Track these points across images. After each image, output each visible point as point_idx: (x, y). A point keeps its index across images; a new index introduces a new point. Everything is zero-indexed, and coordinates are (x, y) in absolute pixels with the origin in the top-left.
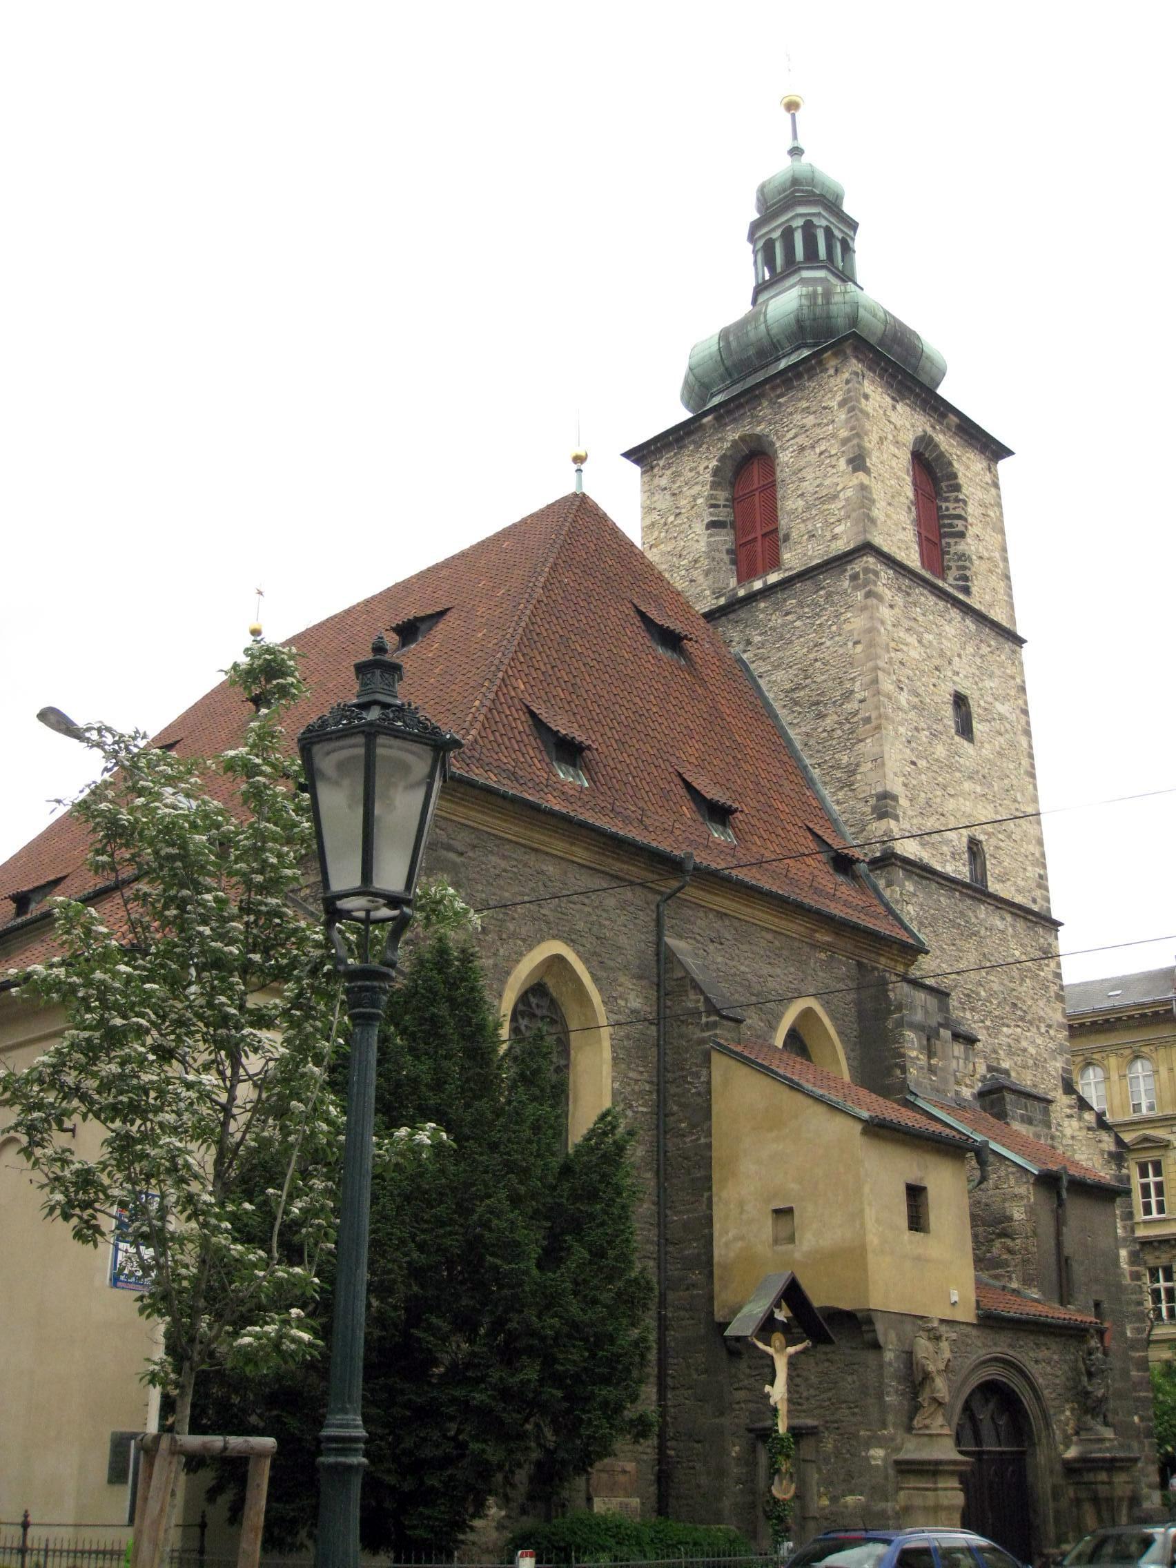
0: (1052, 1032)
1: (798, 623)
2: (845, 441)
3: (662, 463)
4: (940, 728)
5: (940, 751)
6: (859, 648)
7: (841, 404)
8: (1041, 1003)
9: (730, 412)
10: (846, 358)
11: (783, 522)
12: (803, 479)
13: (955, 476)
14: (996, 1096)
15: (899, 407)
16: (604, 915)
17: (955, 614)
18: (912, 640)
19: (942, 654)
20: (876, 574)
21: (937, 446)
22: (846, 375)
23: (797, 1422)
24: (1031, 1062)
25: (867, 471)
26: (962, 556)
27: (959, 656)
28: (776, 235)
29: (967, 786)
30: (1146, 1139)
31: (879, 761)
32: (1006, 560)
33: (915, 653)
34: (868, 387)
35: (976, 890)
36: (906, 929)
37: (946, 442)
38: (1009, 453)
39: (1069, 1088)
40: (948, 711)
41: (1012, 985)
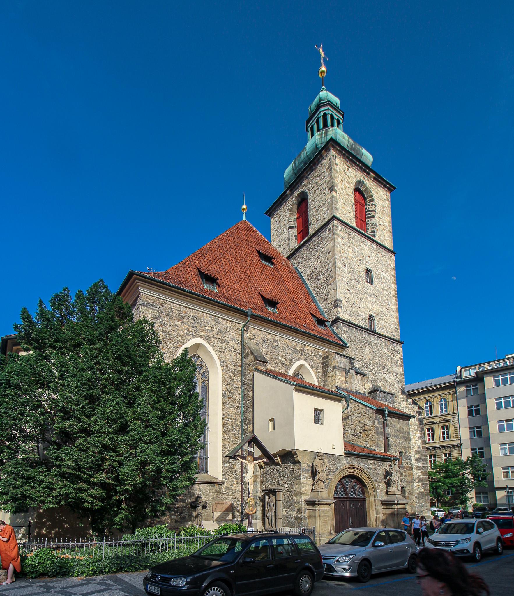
4: (360, 279)
6: (331, 253)
17: (368, 242)
27: (369, 257)
29: (369, 299)
31: (335, 289)
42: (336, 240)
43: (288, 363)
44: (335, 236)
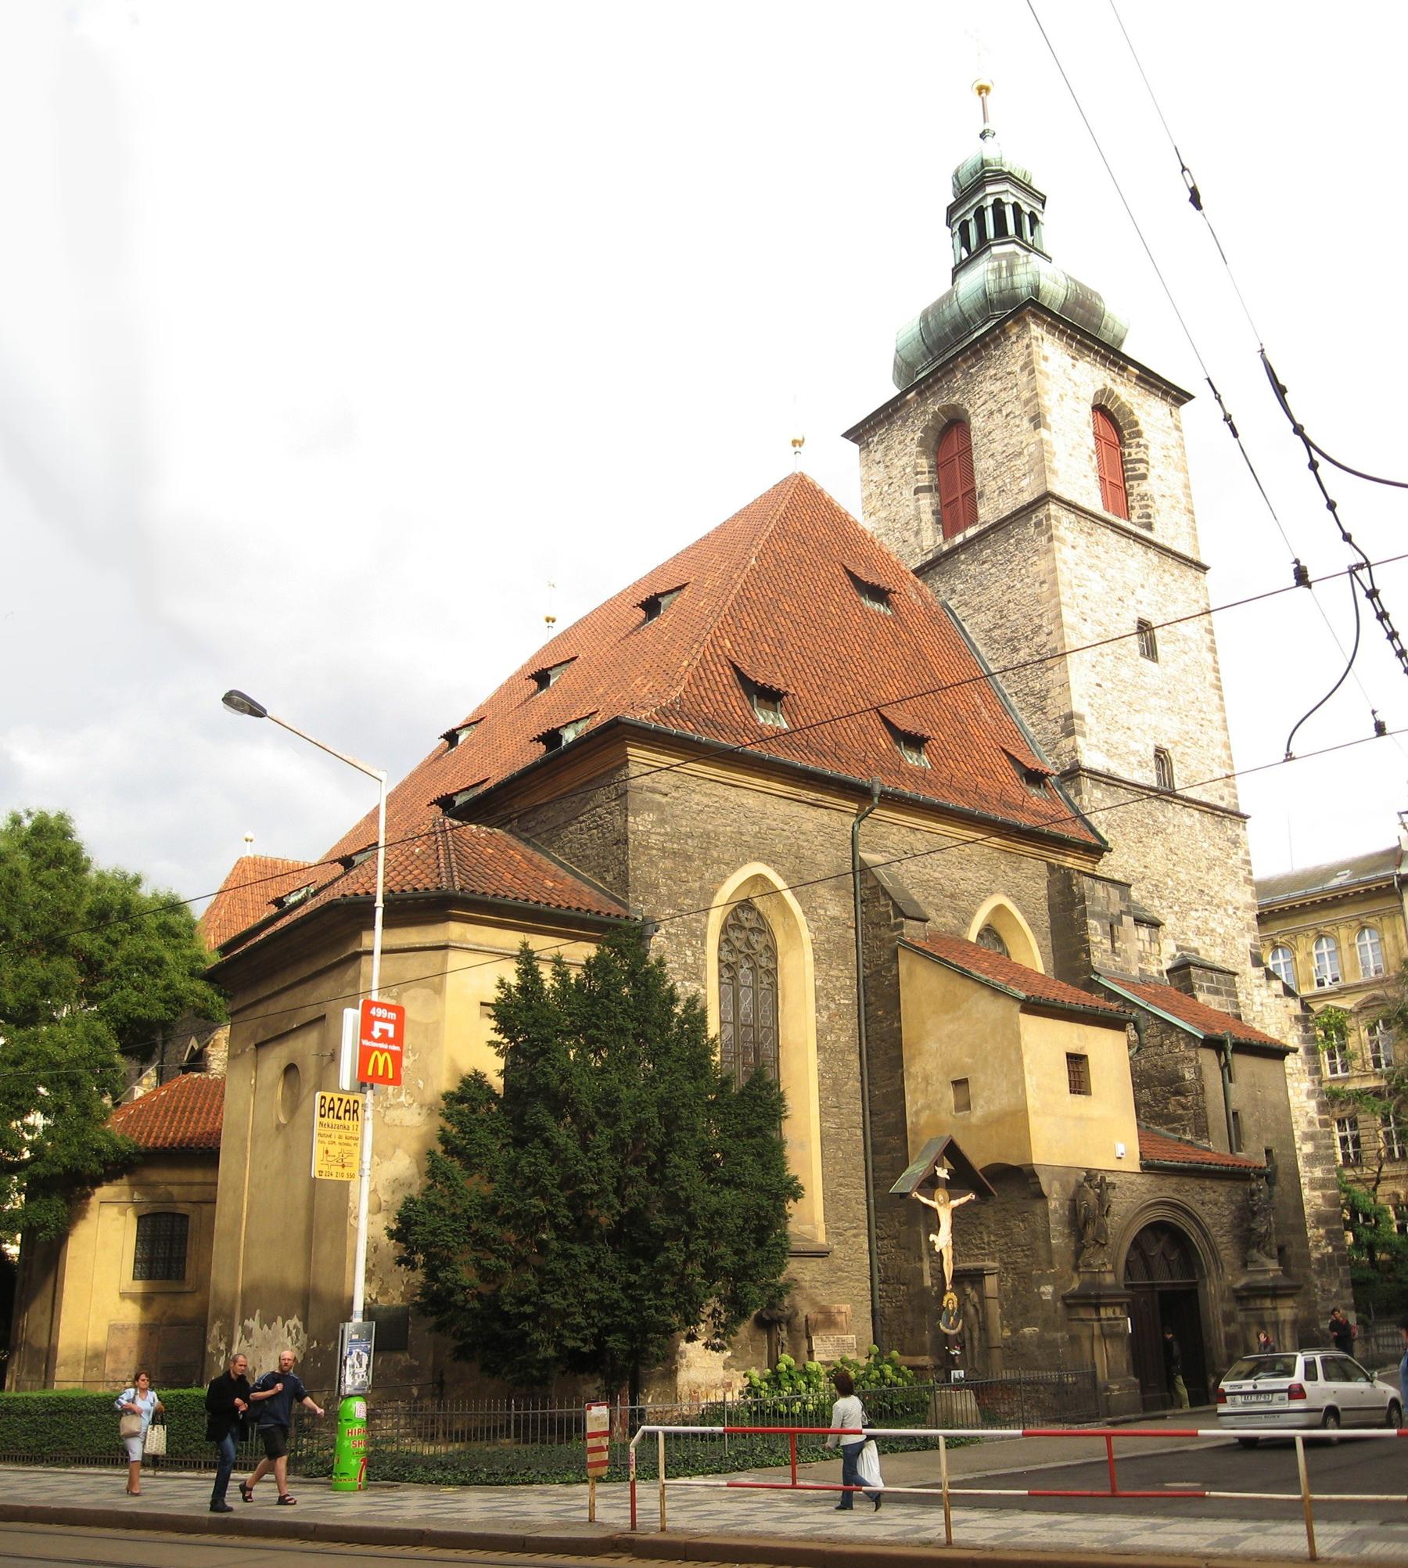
0: (1239, 913)
1: (993, 570)
2: (1027, 402)
3: (876, 439)
4: (1124, 652)
5: (1125, 673)
6: (1045, 586)
7: (1023, 369)
8: (1228, 888)
9: (929, 387)
10: (1027, 325)
12: (991, 442)
13: (1136, 424)
14: (1183, 971)
15: (1080, 364)
16: (803, 837)
17: (1137, 548)
18: (1094, 575)
22: (1026, 341)
23: (962, 1265)
24: (1219, 941)
25: (1048, 427)
27: (1143, 586)
28: (970, 216)
29: (1153, 701)
30: (1375, 998)
31: (1065, 685)
32: (1189, 496)
33: (1096, 587)
35: (1165, 793)
36: (1093, 830)
38: (1191, 397)
39: (1257, 961)
41: (1199, 874)
42: (1058, 555)
44: (1056, 543)
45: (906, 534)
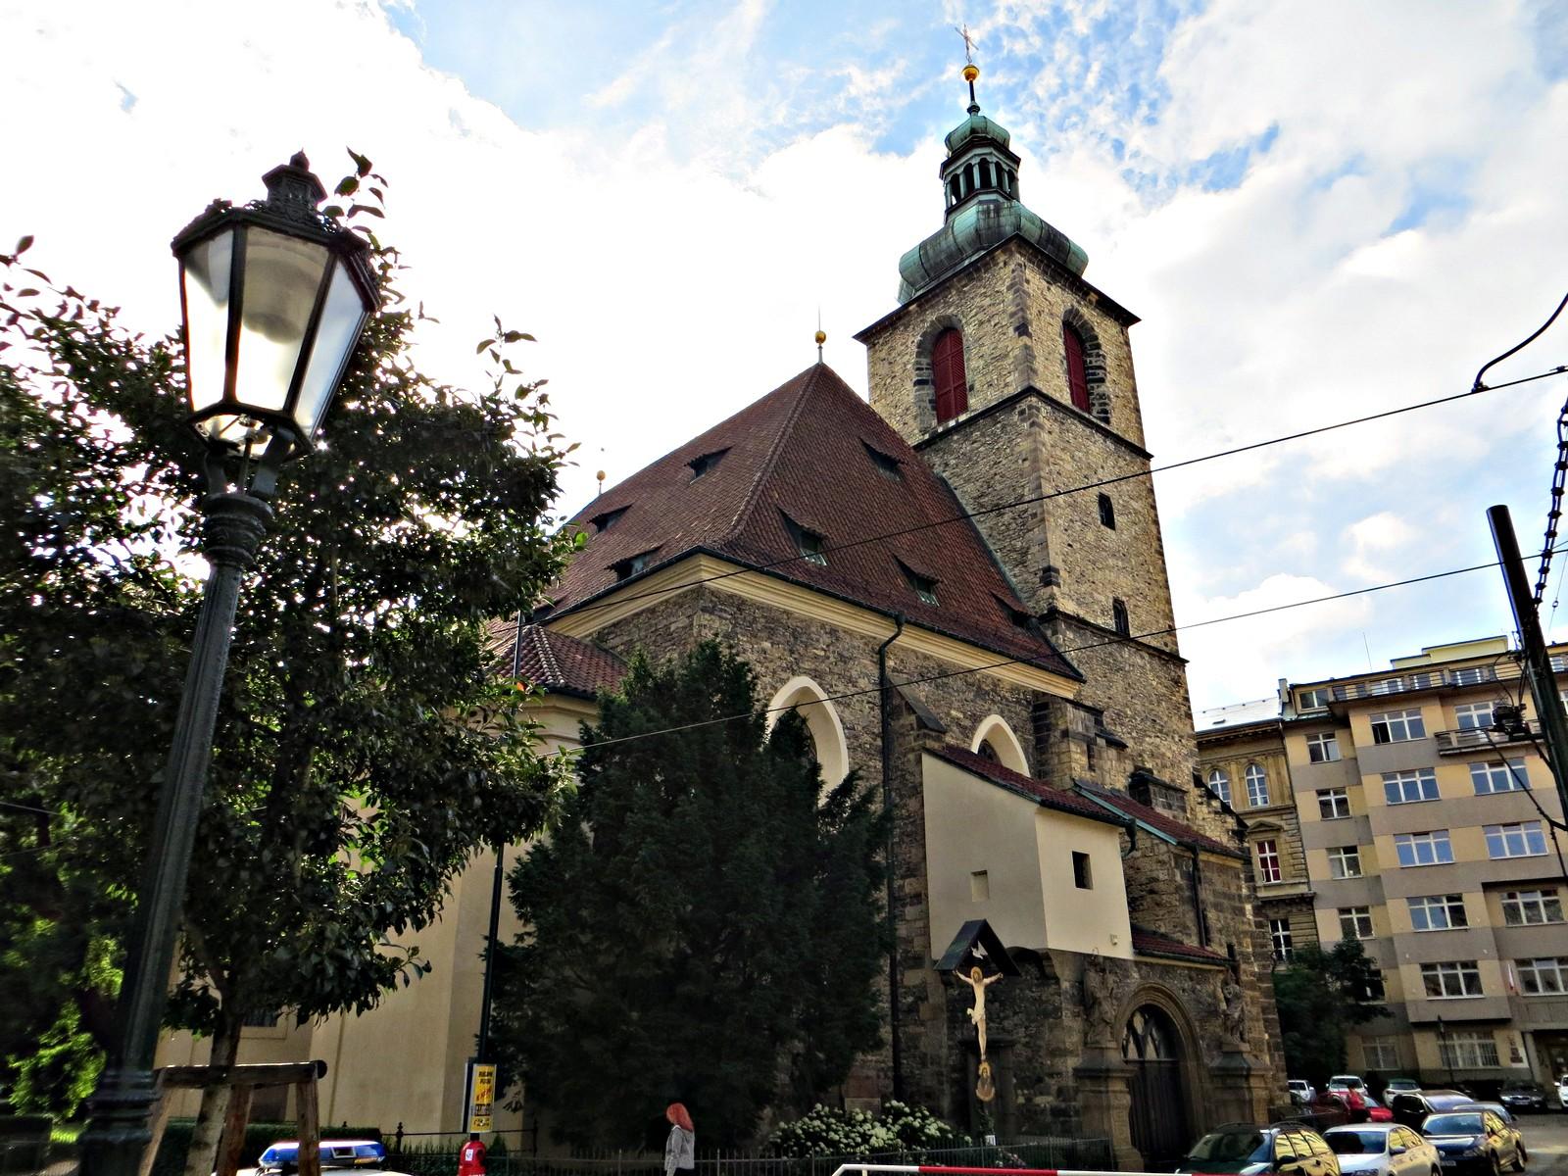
2: (1012, 315)
5: (1090, 537)
6: (1027, 463)
7: (1009, 288)
9: (927, 301)
10: (1011, 255)
11: (969, 376)
13: (1096, 338)
17: (1098, 437)
19: (1089, 467)
20: (1038, 409)
21: (1082, 316)
25: (1030, 335)
26: (1102, 396)
28: (960, 171)
29: (1111, 562)
30: (1262, 824)
31: (1044, 544)
34: (1029, 274)
35: (1121, 635)
37: (1089, 314)
39: (1198, 782)
40: (1095, 509)
43: (967, 723)
45: (907, 418)
